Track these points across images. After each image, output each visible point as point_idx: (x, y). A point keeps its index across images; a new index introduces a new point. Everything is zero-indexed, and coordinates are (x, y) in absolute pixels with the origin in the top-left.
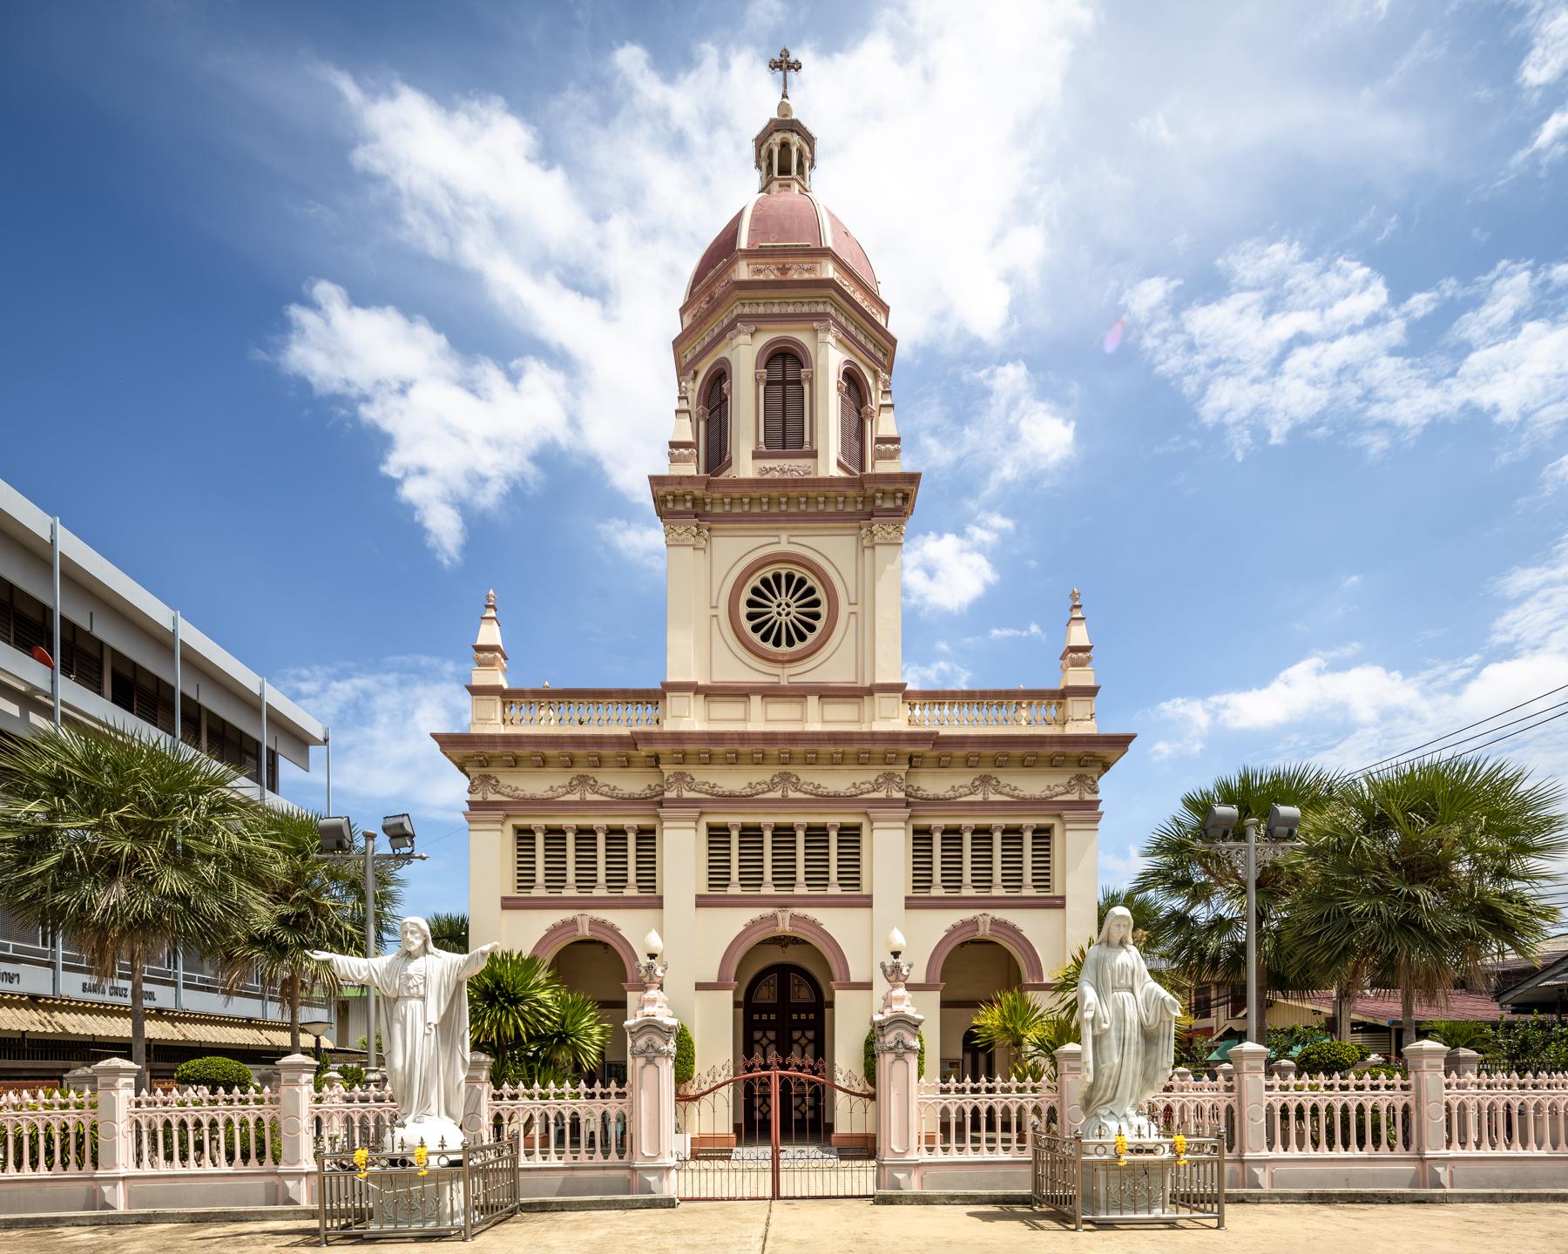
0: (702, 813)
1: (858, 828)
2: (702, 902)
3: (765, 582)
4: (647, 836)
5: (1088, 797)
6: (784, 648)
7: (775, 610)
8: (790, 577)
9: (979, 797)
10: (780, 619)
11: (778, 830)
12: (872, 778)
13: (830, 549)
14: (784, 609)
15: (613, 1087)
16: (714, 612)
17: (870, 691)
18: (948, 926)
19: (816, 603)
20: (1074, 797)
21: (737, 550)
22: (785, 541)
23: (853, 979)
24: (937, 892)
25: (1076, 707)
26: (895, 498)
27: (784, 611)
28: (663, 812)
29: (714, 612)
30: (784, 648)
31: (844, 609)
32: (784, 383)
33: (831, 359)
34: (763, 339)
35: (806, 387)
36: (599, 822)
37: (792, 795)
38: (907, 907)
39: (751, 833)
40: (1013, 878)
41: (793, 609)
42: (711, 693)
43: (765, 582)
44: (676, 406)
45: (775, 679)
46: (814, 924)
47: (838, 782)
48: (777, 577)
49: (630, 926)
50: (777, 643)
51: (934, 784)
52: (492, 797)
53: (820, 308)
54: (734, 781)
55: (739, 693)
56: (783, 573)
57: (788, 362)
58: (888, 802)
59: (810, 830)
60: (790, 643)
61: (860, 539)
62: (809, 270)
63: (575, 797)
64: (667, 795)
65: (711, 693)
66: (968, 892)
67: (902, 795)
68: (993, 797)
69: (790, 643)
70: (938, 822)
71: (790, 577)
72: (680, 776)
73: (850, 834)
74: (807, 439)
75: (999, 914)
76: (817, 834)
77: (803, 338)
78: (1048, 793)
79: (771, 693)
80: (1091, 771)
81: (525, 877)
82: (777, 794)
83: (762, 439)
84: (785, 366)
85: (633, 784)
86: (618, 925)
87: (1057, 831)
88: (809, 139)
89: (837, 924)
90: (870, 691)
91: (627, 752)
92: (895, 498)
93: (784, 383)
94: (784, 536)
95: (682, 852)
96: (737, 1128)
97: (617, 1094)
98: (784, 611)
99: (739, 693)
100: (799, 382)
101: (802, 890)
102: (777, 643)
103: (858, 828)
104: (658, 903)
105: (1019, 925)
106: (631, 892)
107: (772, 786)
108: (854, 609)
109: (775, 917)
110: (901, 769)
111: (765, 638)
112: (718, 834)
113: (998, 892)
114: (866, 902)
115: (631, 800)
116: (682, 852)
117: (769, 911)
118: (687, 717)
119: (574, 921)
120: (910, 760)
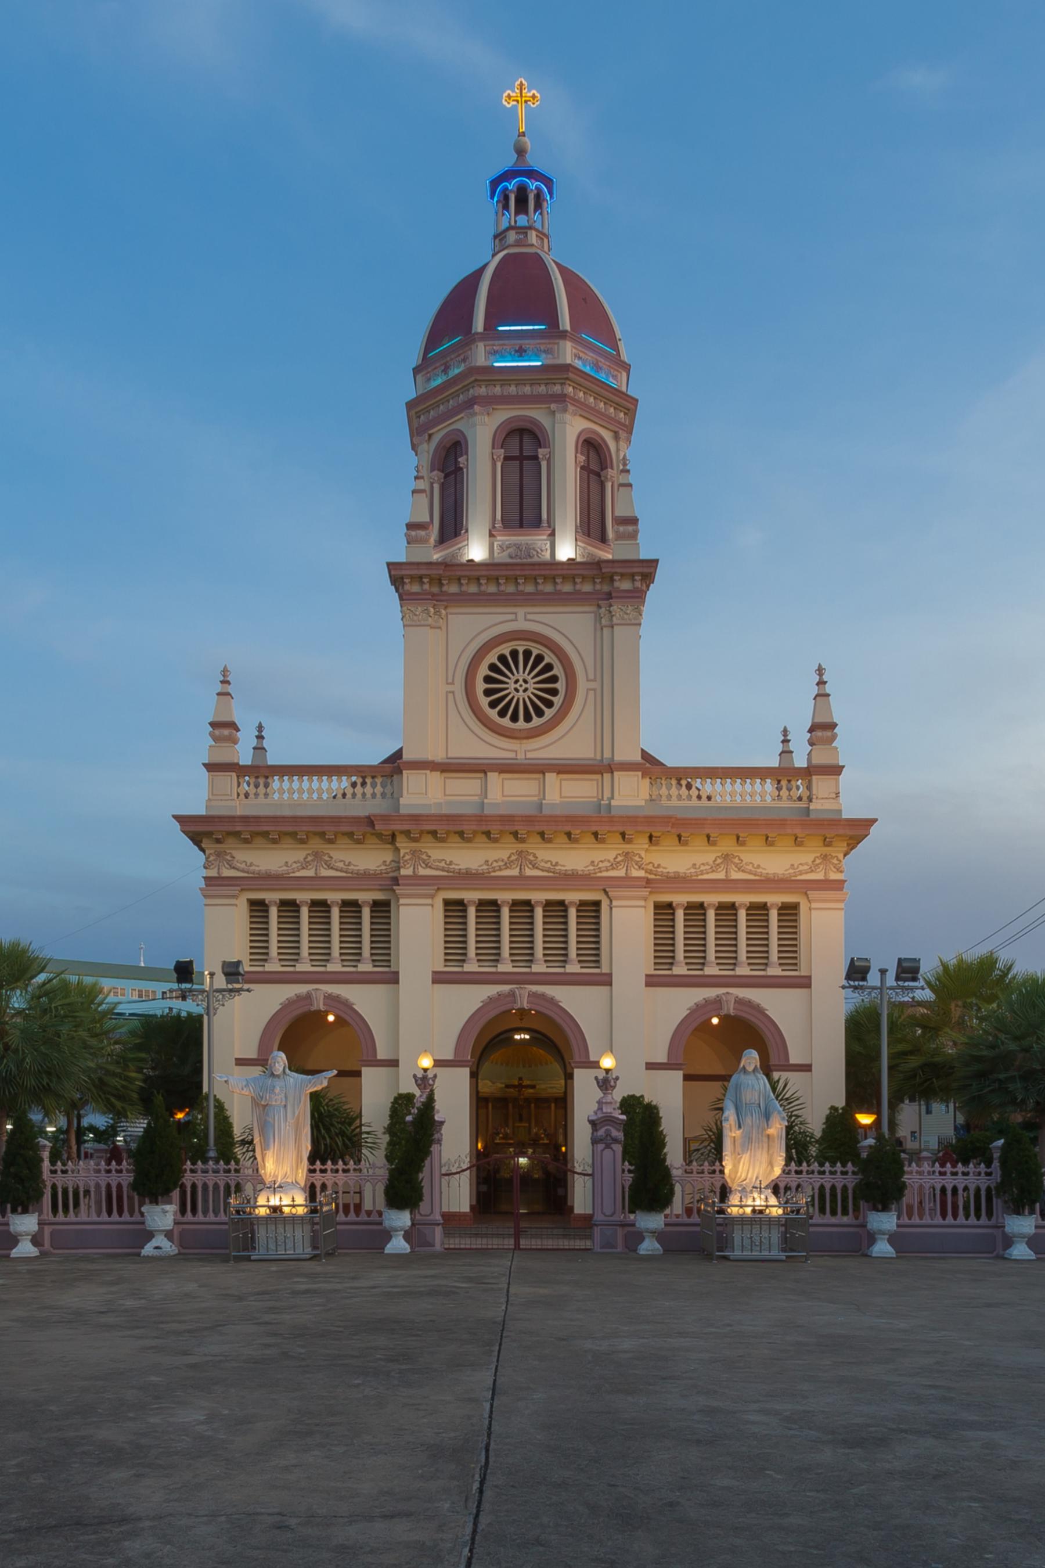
0: (438, 889)
1: (597, 904)
2: (439, 978)
3: (502, 658)
4: (382, 909)
5: (834, 876)
6: (521, 724)
7: (513, 686)
8: (527, 654)
9: (721, 876)
10: (517, 695)
11: (515, 905)
12: (611, 855)
13: (569, 627)
14: (521, 685)
15: (351, 1165)
16: (450, 688)
18: (691, 1004)
19: (554, 679)
20: (819, 876)
21: (473, 627)
24: (680, 970)
25: (821, 785)
26: (634, 580)
27: (521, 687)
28: (398, 890)
29: (450, 688)
30: (521, 724)
31: (582, 685)
32: (521, 458)
33: (568, 430)
34: (502, 415)
36: (334, 897)
37: (529, 872)
38: (647, 986)
40: (759, 955)
41: (531, 686)
43: (502, 658)
44: (413, 485)
45: (512, 755)
46: (553, 1002)
47: (575, 859)
48: (514, 654)
50: (514, 718)
51: (674, 860)
52: (227, 873)
53: (557, 389)
54: (469, 858)
55: (479, 768)
56: (521, 650)
57: (527, 440)
58: (627, 882)
59: (548, 904)
60: (528, 718)
61: (598, 618)
62: (547, 352)
63: (310, 873)
64: (403, 872)
66: (712, 970)
67: (641, 874)
68: (735, 875)
69: (528, 718)
70: (680, 899)
71: (527, 654)
73: (591, 910)
74: (544, 516)
76: (556, 909)
78: (791, 871)
80: (837, 850)
81: (260, 952)
82: (515, 872)
83: (499, 516)
84: (523, 447)
85: (370, 859)
87: (803, 909)
88: (548, 182)
89: (577, 1003)
91: (367, 829)
92: (634, 580)
93: (521, 458)
94: (521, 611)
96: (472, 1207)
97: (355, 1170)
98: (521, 687)
99: (479, 768)
100: (535, 458)
101: (539, 967)
102: (514, 718)
103: (597, 904)
104: (393, 979)
105: (764, 1005)
106: (366, 967)
107: (507, 865)
108: (592, 685)
109: (512, 994)
110: (640, 845)
111: (502, 714)
112: (455, 908)
113: (743, 970)
114: (606, 980)
115: (363, 879)
117: (506, 988)
118: (422, 793)
119: (308, 996)
120: (651, 837)
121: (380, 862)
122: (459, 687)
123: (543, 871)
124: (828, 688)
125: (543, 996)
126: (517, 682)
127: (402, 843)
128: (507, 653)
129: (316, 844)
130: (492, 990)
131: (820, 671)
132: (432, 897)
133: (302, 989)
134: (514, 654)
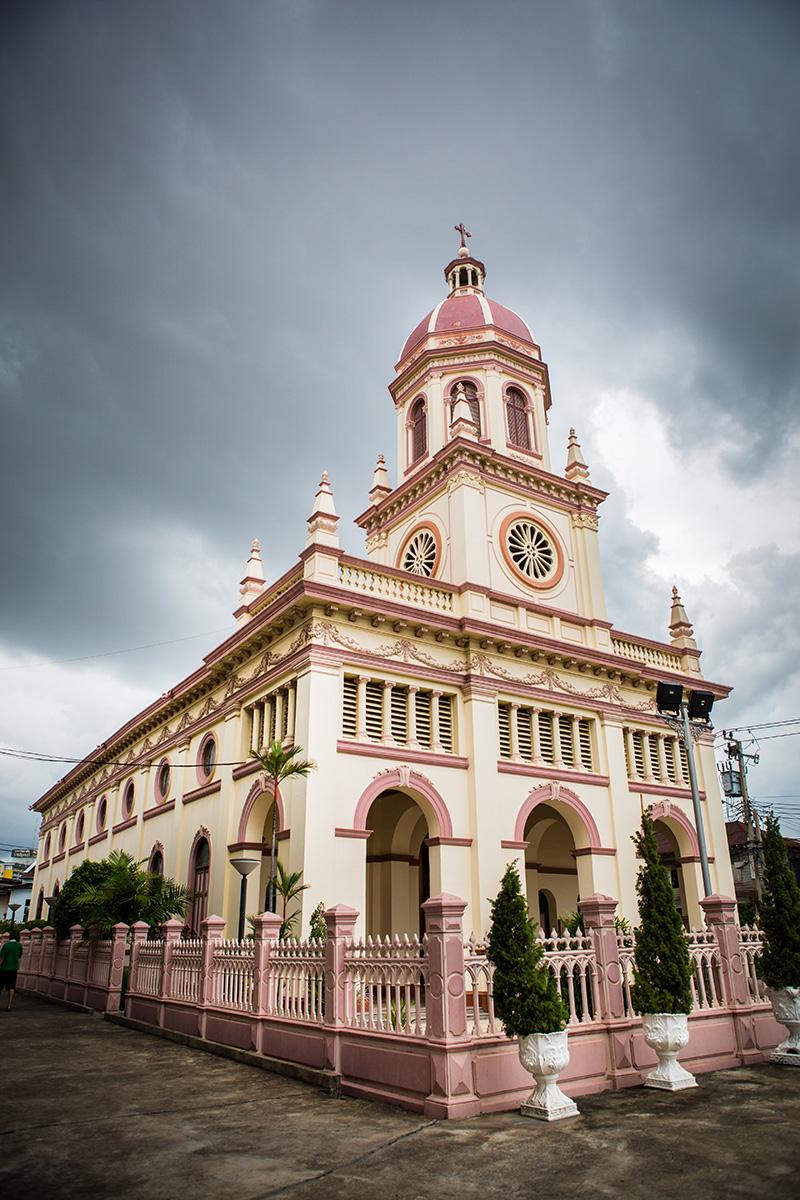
1: (593, 720)
13: (557, 521)
16: (490, 539)
17: (592, 623)
22: (529, 507)
23: (603, 847)
29: (490, 539)
35: (530, 416)
39: (525, 713)
41: (536, 551)
42: (496, 598)
47: (583, 685)
48: (525, 527)
49: (444, 783)
54: (519, 671)
55: (514, 604)
56: (529, 526)
65: (496, 598)
72: (481, 658)
74: (533, 445)
75: (674, 801)
77: (527, 388)
79: (533, 609)
85: (445, 657)
86: (431, 780)
90: (592, 623)
94: (528, 502)
95: (478, 720)
99: (514, 604)
103: (593, 720)
112: (504, 708)
116: (478, 720)
121: (452, 662)
122: (496, 540)
123: (563, 689)
124: (682, 602)
125: (566, 790)
126: (528, 547)
127: (473, 647)
128: (521, 525)
129: (407, 635)
130: (537, 782)
131: (675, 590)
132: (494, 696)
133: (393, 765)
134: (525, 527)
